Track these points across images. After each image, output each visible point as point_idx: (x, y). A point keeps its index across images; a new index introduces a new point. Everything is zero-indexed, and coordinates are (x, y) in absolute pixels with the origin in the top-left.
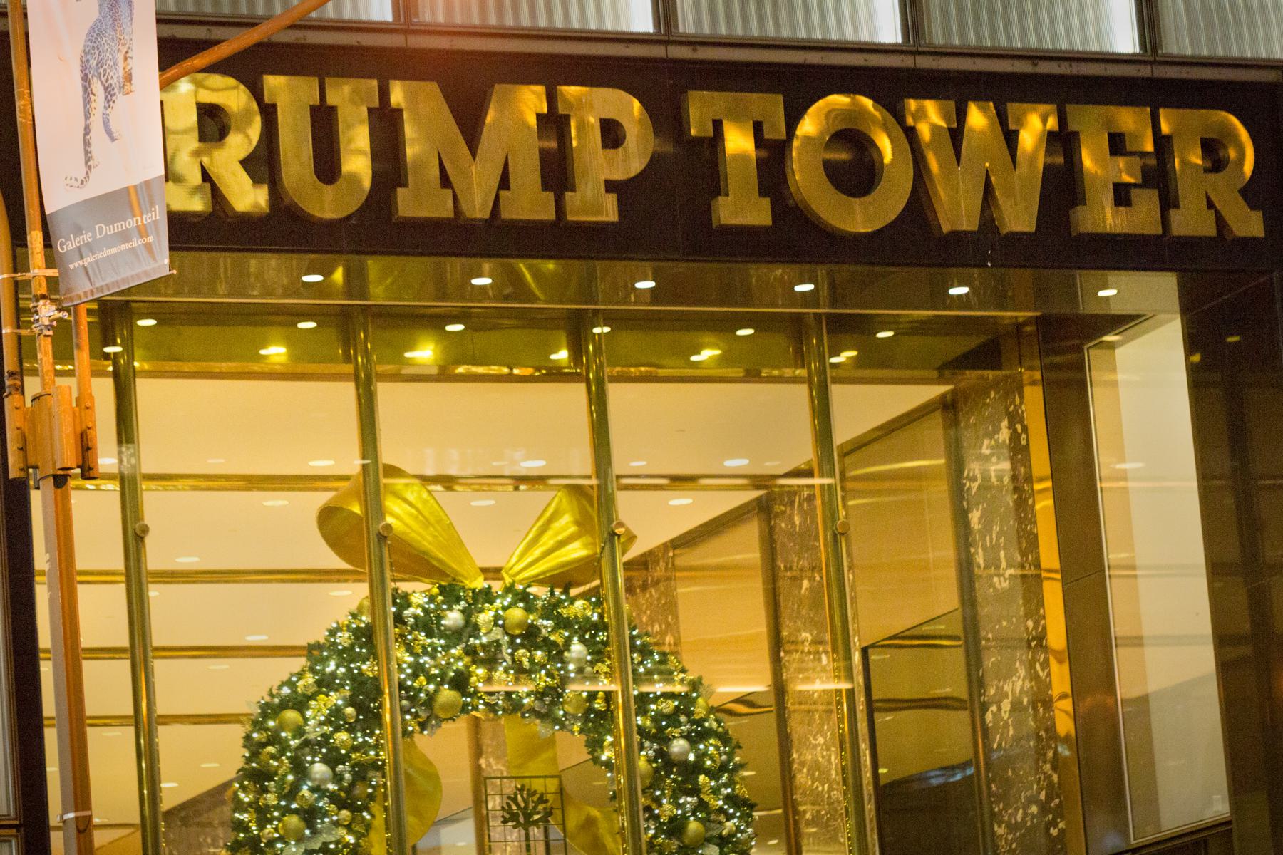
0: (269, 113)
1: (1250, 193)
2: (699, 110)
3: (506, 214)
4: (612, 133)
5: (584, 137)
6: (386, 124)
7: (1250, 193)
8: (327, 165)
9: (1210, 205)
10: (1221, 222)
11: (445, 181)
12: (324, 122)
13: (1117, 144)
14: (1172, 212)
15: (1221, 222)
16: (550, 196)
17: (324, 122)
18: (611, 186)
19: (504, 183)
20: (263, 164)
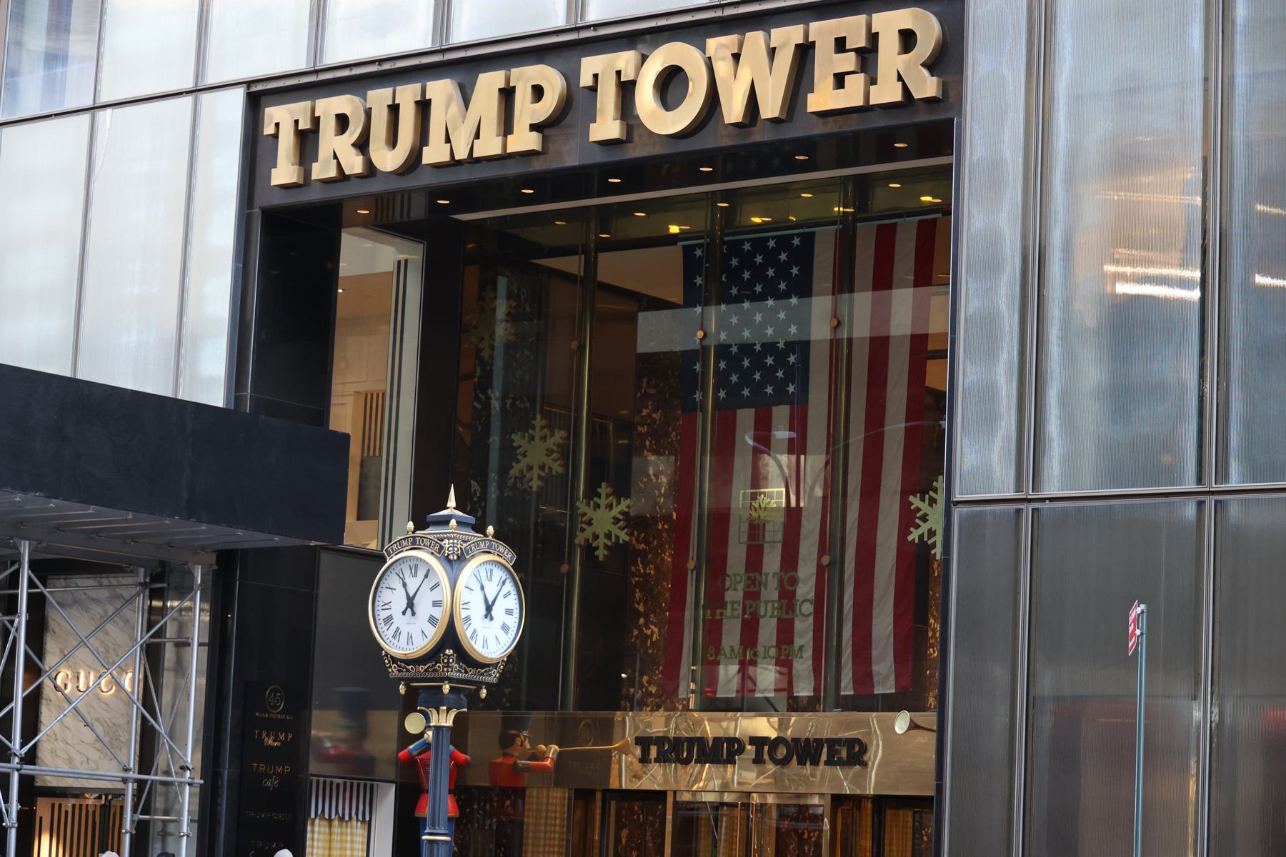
0: (368, 113)
1: (932, 65)
2: (590, 66)
3: (475, 155)
4: (538, 92)
5: (523, 96)
6: (423, 106)
7: (932, 65)
8: (393, 141)
9: (900, 78)
10: (906, 90)
11: (448, 140)
12: (394, 109)
13: (840, 45)
14: (872, 88)
15: (906, 90)
16: (500, 138)
17: (394, 109)
18: (534, 127)
19: (477, 136)
20: (362, 145)
